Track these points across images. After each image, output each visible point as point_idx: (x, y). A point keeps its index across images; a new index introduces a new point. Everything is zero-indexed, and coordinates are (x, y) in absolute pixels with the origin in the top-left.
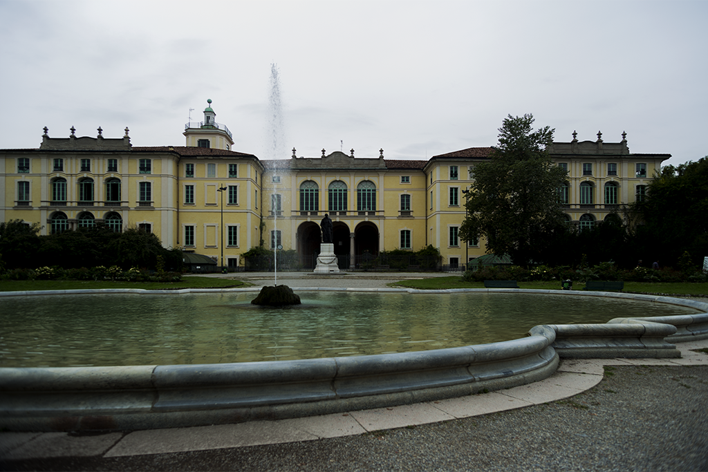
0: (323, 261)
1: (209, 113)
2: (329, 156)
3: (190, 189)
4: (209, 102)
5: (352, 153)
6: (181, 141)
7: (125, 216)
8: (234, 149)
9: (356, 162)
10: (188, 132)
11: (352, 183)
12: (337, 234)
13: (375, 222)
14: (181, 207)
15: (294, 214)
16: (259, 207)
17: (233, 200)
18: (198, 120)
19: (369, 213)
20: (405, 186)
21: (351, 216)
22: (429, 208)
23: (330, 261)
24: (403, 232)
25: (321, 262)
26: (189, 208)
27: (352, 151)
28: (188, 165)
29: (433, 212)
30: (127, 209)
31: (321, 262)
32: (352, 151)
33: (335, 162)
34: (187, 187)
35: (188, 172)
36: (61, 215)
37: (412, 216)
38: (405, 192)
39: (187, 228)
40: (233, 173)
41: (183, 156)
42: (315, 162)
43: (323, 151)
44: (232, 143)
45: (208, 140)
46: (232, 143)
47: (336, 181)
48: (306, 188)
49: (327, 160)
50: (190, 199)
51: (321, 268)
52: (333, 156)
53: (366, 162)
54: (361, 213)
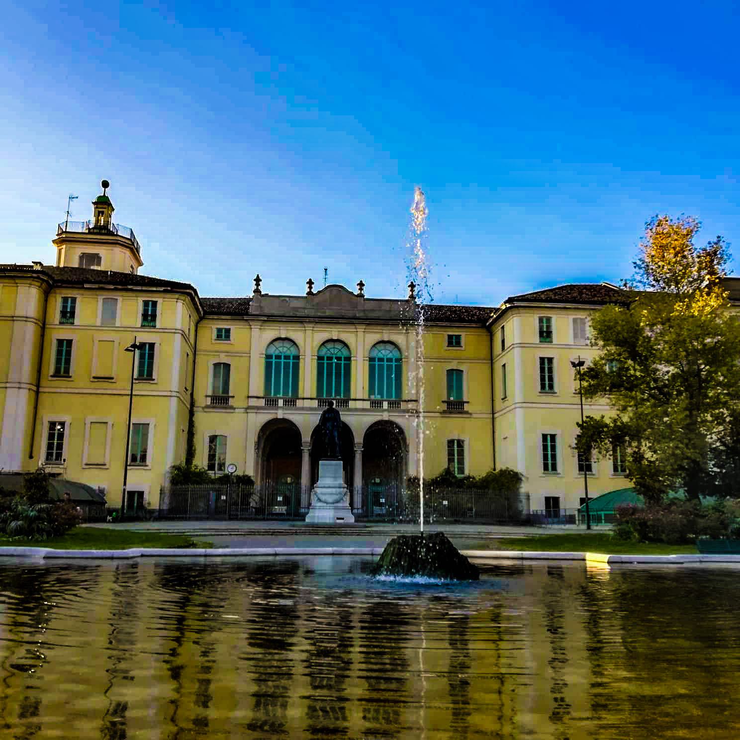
0: (323, 498)
1: (103, 204)
2: (319, 292)
3: (65, 347)
4: (105, 184)
5: (361, 289)
6: (49, 256)
8: (141, 272)
9: (368, 306)
10: (65, 238)
11: (361, 342)
12: (332, 438)
13: (399, 419)
14: (43, 383)
15: (253, 402)
16: (189, 388)
17: (146, 373)
18: (84, 217)
19: (390, 403)
20: (454, 351)
21: (356, 410)
22: (499, 394)
23: (336, 497)
24: (451, 443)
25: (319, 500)
26: (61, 383)
27: (361, 285)
28: (65, 300)
29: (507, 403)
31: (319, 500)
32: (361, 285)
33: (331, 305)
34: (60, 342)
35: (64, 313)
37: (467, 413)
38: (454, 365)
40: (149, 317)
41: (59, 281)
42: (295, 304)
43: (310, 283)
44: (140, 264)
45: (97, 254)
46: (140, 264)
47: (331, 341)
48: (277, 353)
49: (316, 300)
51: (322, 514)
52: (327, 294)
53: (386, 307)
54: (376, 405)
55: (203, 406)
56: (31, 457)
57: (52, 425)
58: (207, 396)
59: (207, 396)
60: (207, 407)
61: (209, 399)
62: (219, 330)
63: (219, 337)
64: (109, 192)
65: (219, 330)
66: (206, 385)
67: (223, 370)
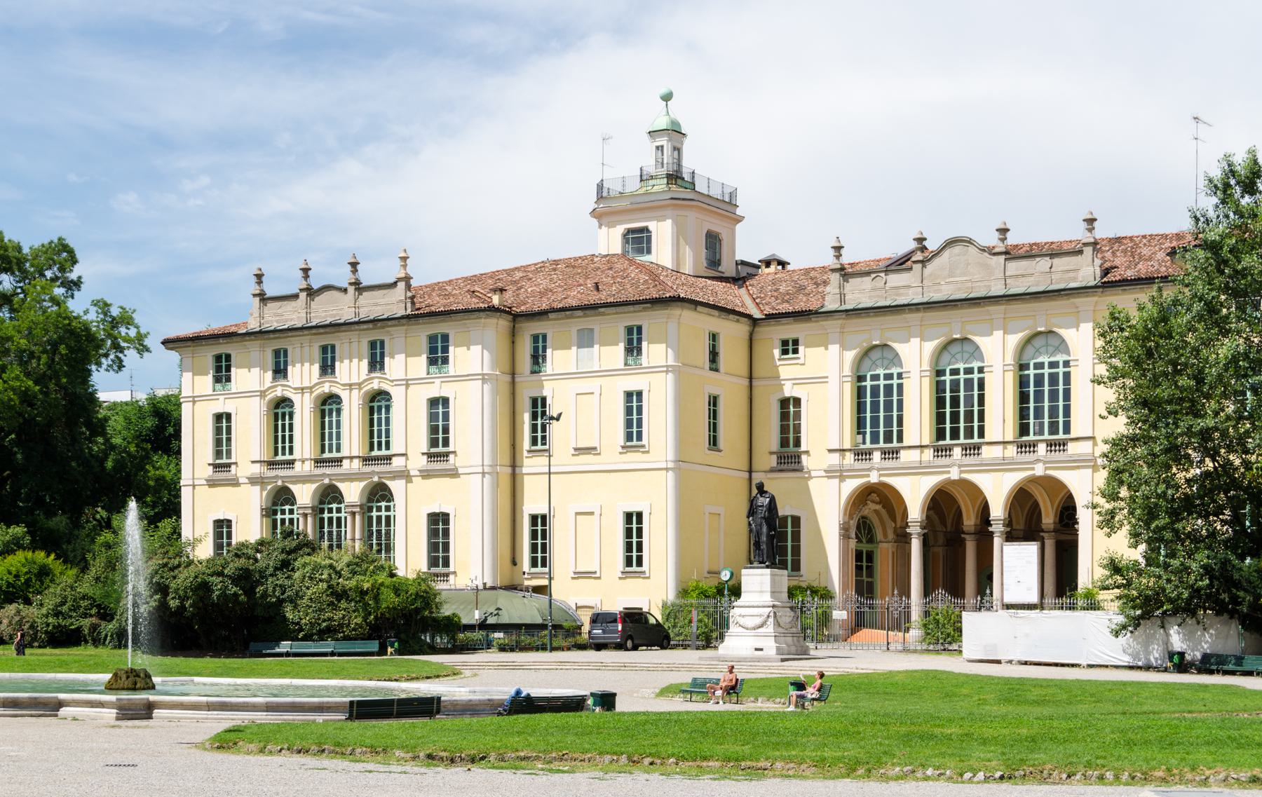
0: (742, 621)
3: (539, 405)
7: (396, 486)
23: (758, 621)
28: (535, 338)
30: (405, 475)
36: (282, 497)
39: (534, 518)
50: (540, 437)
55: (768, 468)
56: (514, 563)
57: (534, 518)
58: (771, 453)
59: (771, 453)
60: (772, 470)
61: (774, 457)
62: (785, 343)
63: (785, 352)
64: (679, 110)
65: (785, 343)
66: (769, 437)
67: (789, 408)
